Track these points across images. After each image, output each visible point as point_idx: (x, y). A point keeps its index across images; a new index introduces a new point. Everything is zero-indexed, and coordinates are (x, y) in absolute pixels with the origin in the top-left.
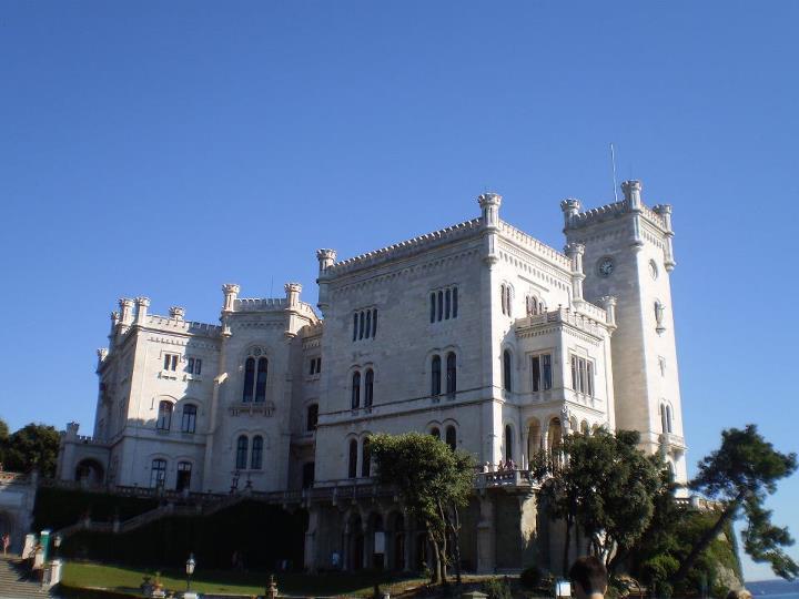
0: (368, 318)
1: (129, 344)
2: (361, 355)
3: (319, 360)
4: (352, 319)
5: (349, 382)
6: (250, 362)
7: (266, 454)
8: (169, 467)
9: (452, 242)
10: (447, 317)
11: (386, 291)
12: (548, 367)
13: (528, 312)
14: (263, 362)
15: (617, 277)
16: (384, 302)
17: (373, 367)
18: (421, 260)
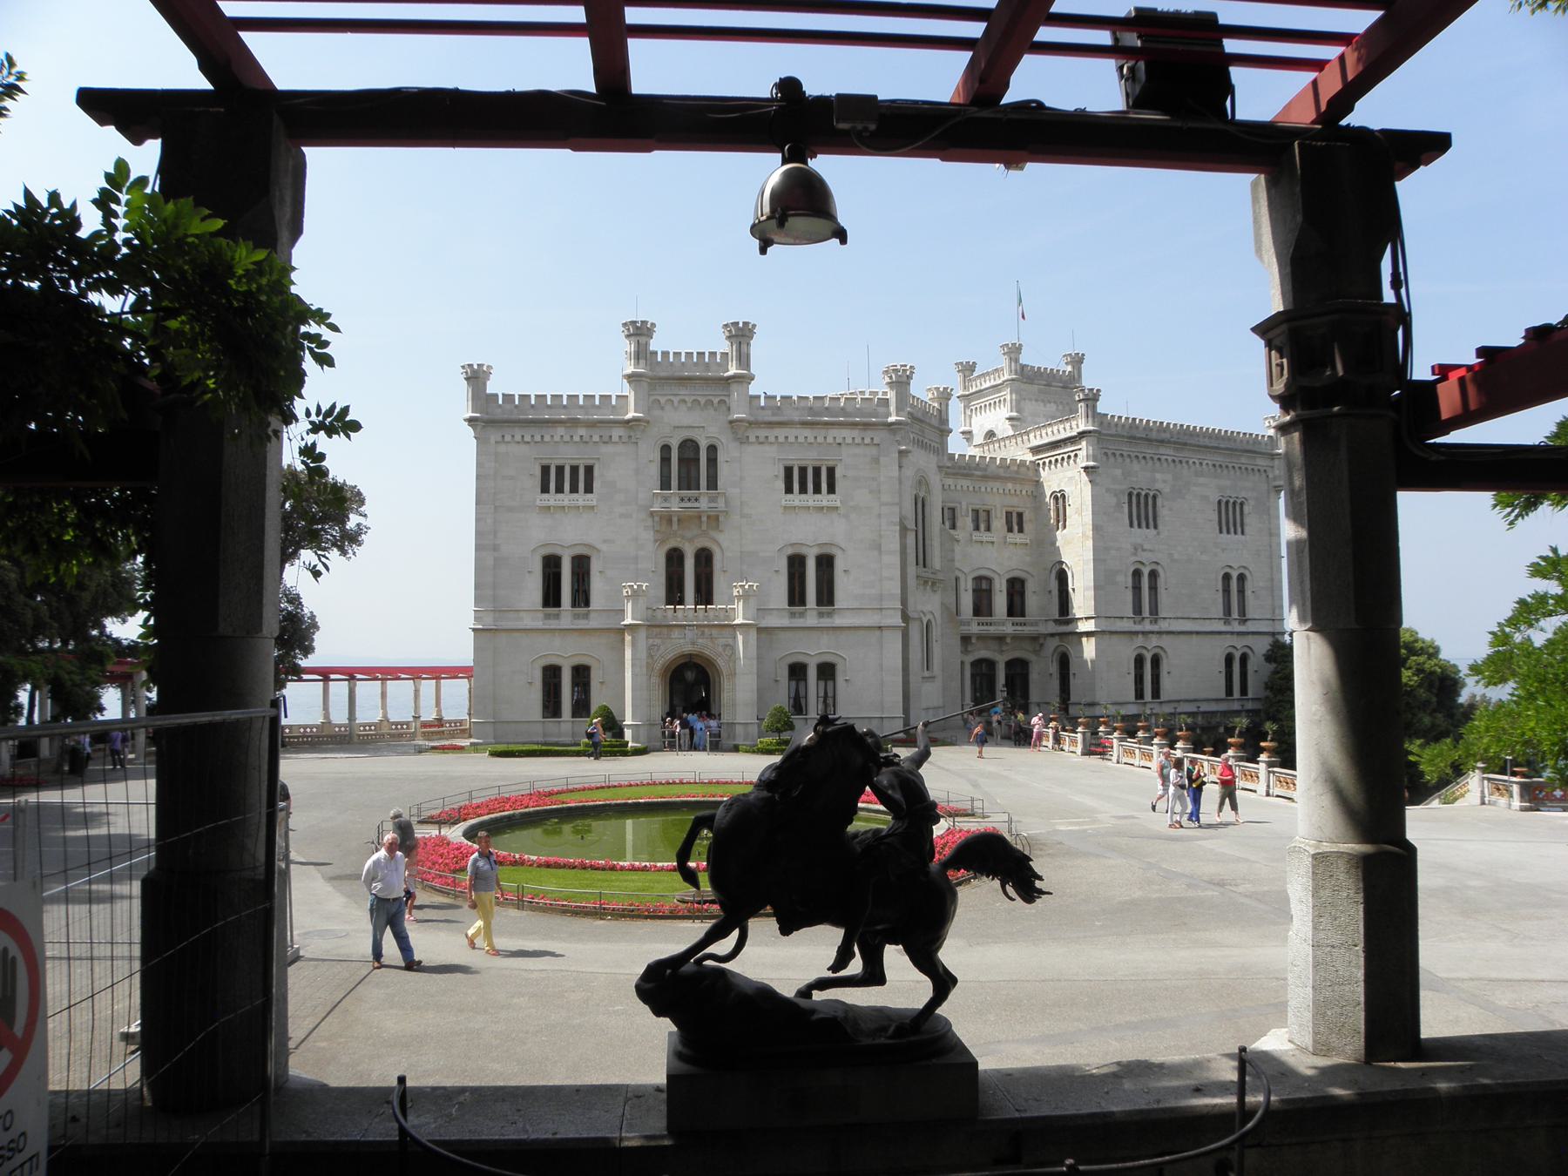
2: (1144, 550)
4: (1126, 499)
11: (1169, 477)
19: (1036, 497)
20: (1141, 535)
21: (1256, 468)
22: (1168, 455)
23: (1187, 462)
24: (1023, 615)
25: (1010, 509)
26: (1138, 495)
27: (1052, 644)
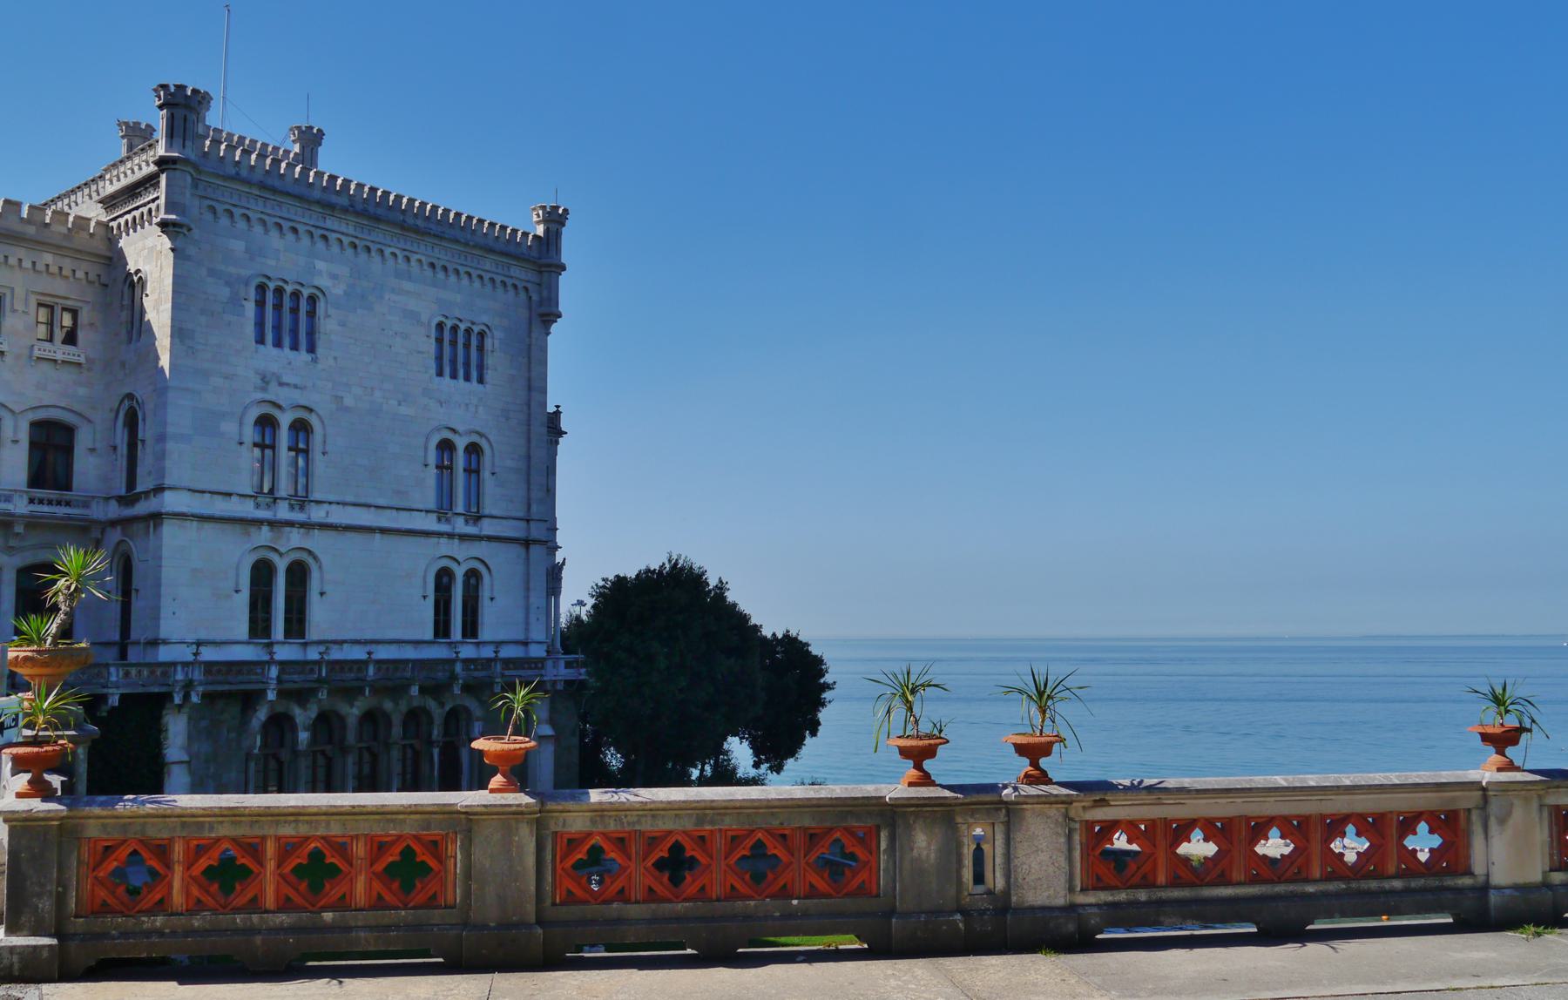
0: (295, 311)
2: (281, 384)
4: (252, 293)
17: (314, 421)
19: (106, 286)
20: (274, 358)
21: (509, 282)
22: (343, 233)
23: (381, 252)
24: (68, 487)
25: (48, 300)
26: (279, 291)
27: (115, 535)
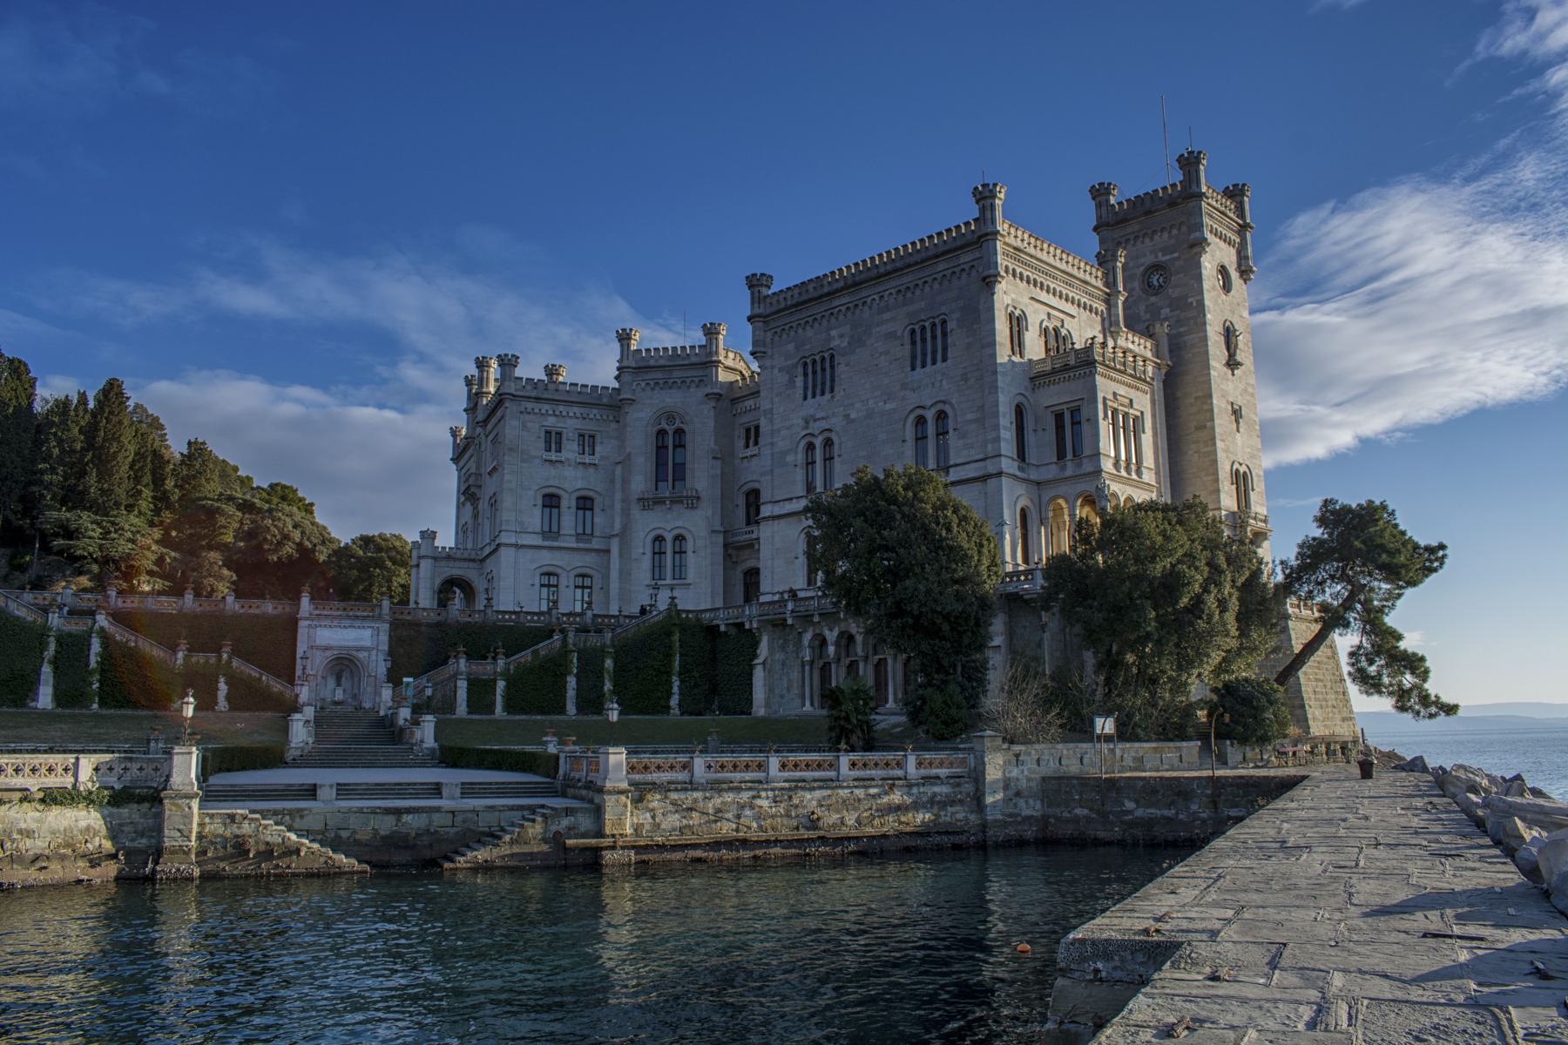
1: (493, 421)
3: (757, 428)
4: (800, 370)
5: (800, 457)
6: (661, 433)
7: (691, 559)
8: (563, 582)
9: (937, 256)
10: (934, 362)
12: (1076, 423)
13: (1047, 350)
14: (680, 432)
15: (1174, 293)
16: (845, 344)
18: (893, 283)
26: (814, 362)
